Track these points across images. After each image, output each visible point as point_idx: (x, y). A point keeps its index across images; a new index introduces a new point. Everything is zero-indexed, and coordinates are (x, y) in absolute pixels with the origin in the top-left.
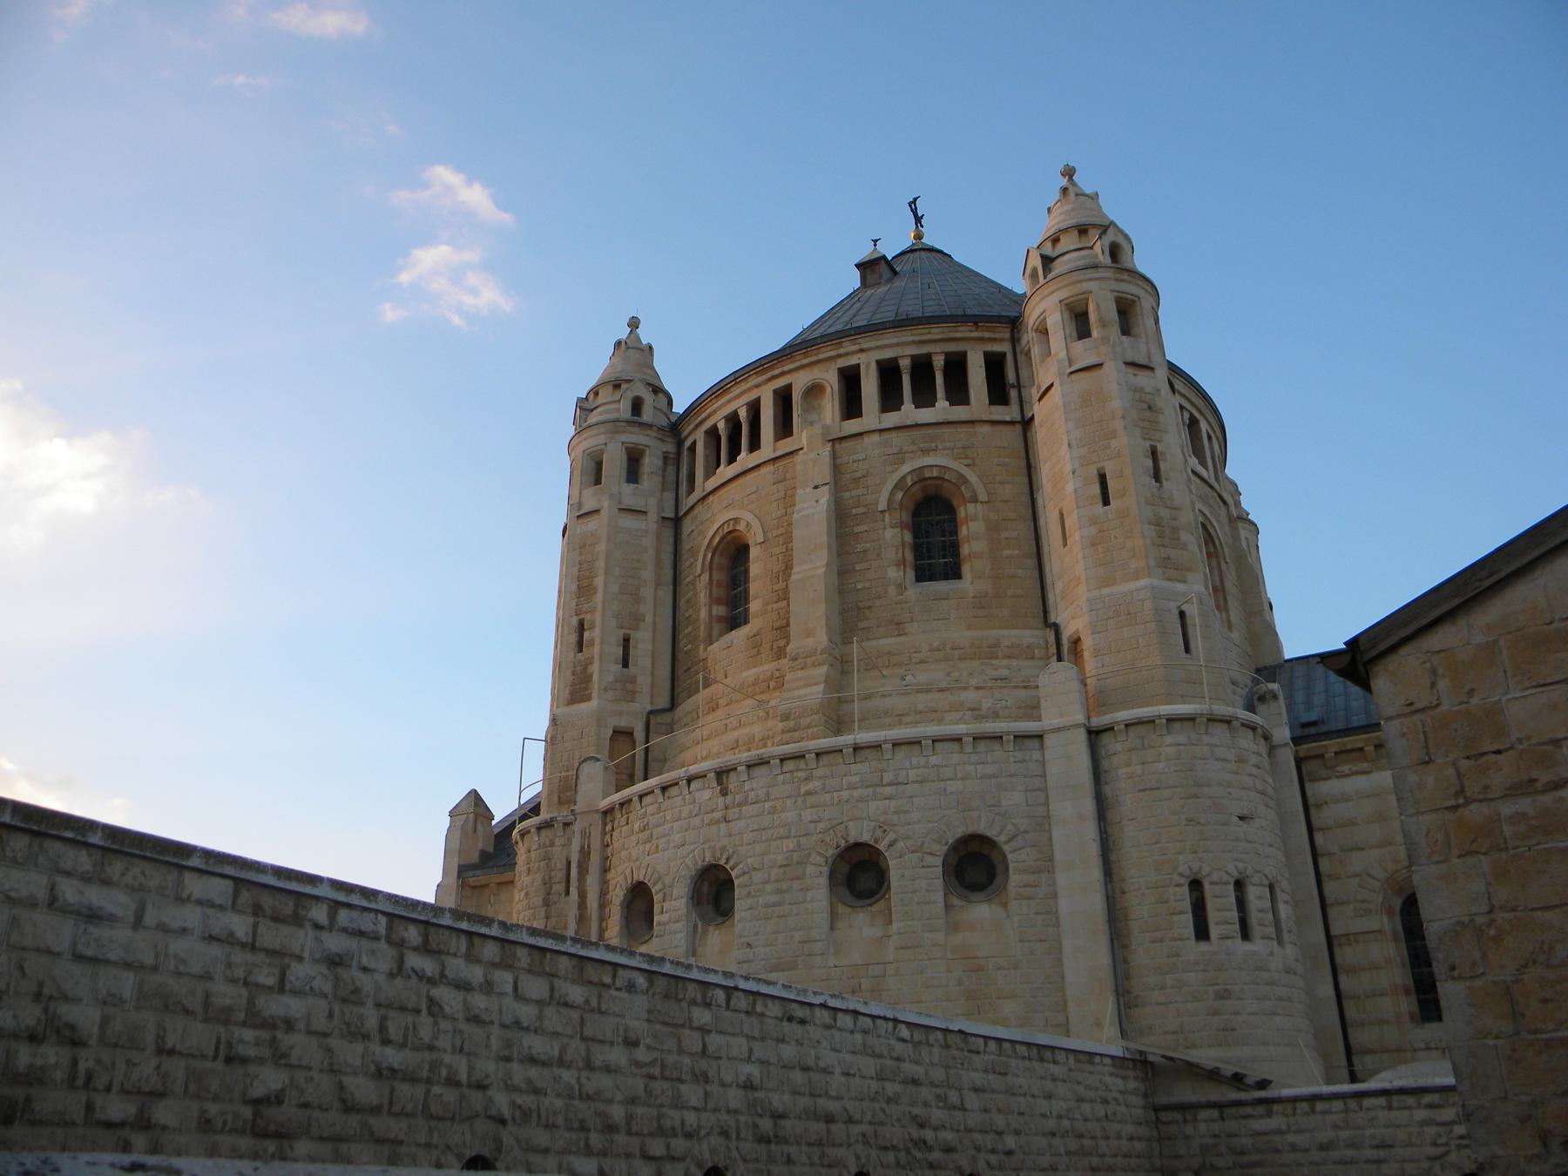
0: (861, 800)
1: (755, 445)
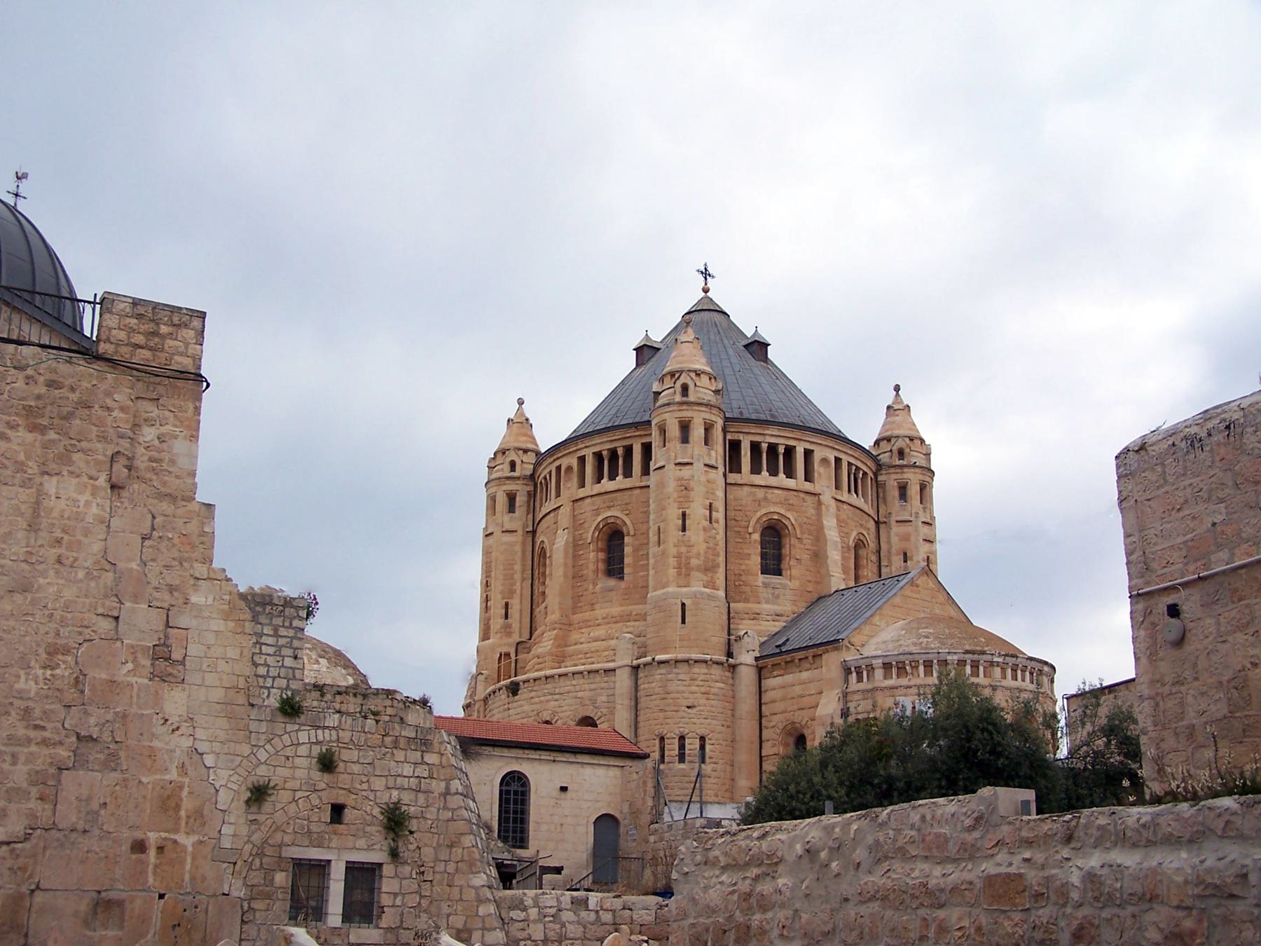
0: (548, 701)
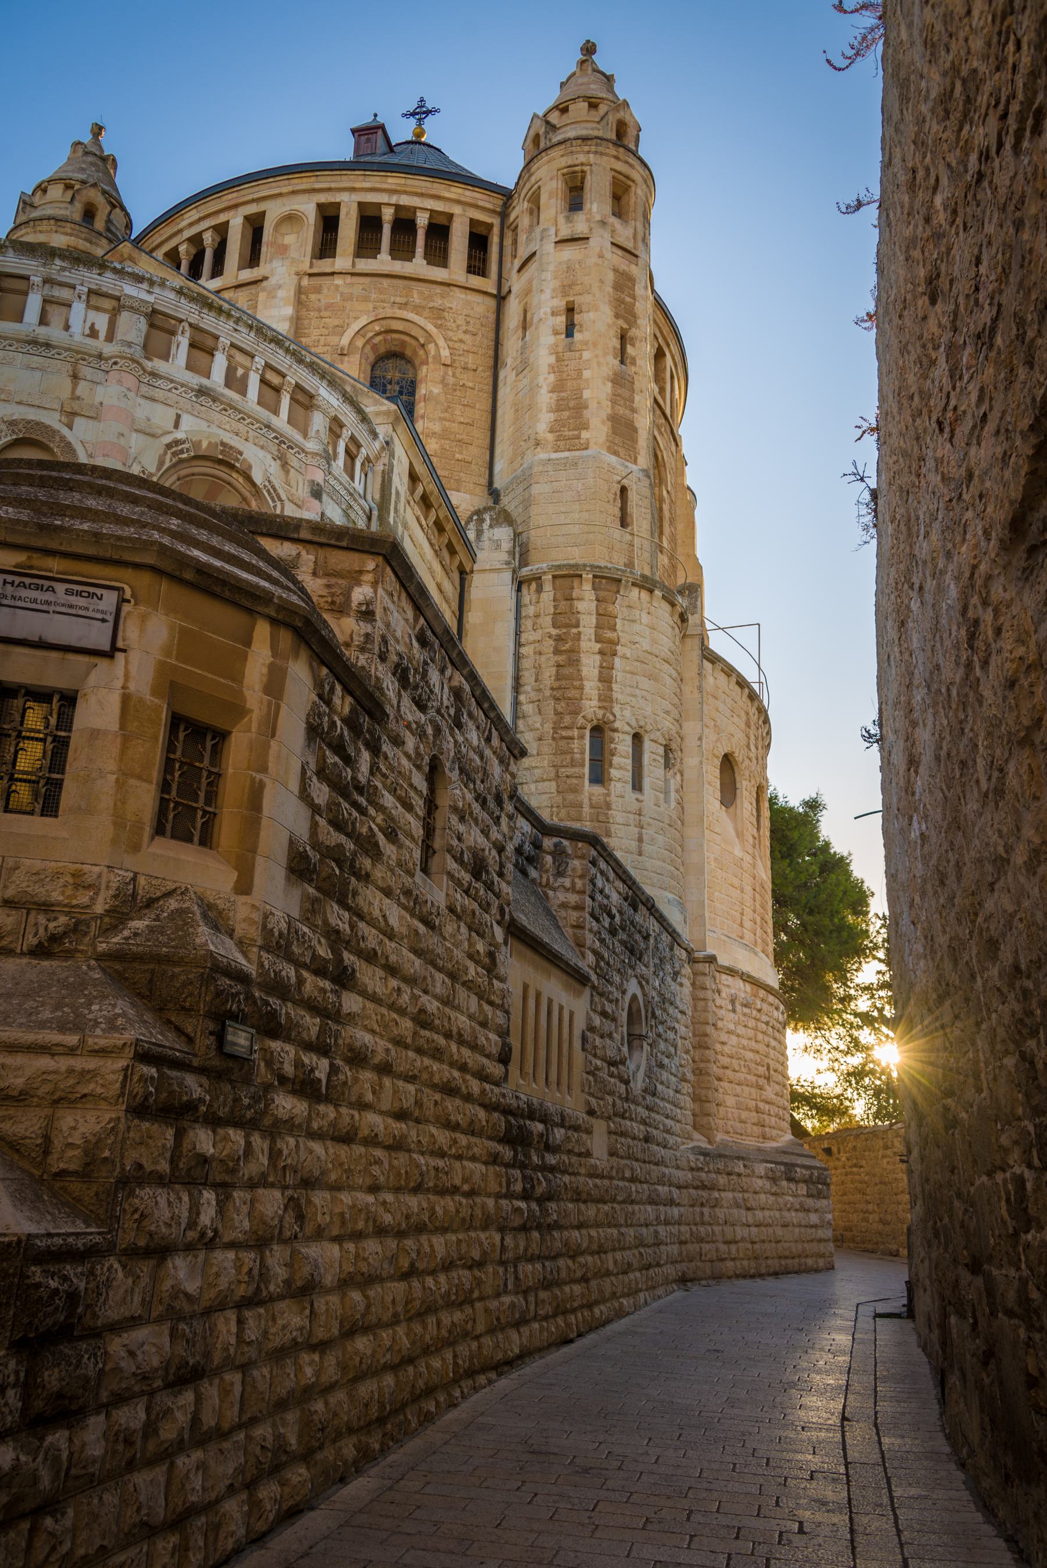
1: (217, 270)
